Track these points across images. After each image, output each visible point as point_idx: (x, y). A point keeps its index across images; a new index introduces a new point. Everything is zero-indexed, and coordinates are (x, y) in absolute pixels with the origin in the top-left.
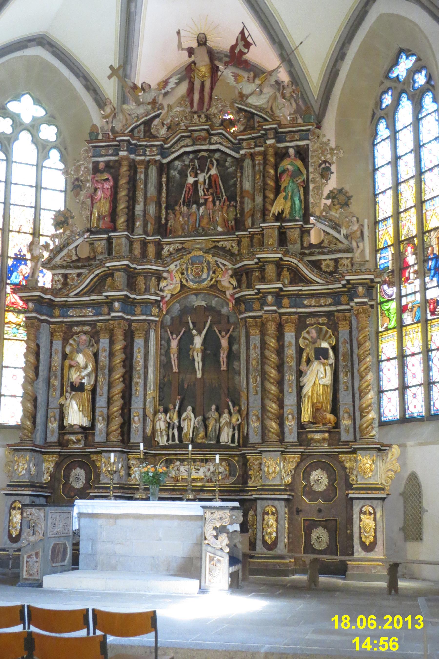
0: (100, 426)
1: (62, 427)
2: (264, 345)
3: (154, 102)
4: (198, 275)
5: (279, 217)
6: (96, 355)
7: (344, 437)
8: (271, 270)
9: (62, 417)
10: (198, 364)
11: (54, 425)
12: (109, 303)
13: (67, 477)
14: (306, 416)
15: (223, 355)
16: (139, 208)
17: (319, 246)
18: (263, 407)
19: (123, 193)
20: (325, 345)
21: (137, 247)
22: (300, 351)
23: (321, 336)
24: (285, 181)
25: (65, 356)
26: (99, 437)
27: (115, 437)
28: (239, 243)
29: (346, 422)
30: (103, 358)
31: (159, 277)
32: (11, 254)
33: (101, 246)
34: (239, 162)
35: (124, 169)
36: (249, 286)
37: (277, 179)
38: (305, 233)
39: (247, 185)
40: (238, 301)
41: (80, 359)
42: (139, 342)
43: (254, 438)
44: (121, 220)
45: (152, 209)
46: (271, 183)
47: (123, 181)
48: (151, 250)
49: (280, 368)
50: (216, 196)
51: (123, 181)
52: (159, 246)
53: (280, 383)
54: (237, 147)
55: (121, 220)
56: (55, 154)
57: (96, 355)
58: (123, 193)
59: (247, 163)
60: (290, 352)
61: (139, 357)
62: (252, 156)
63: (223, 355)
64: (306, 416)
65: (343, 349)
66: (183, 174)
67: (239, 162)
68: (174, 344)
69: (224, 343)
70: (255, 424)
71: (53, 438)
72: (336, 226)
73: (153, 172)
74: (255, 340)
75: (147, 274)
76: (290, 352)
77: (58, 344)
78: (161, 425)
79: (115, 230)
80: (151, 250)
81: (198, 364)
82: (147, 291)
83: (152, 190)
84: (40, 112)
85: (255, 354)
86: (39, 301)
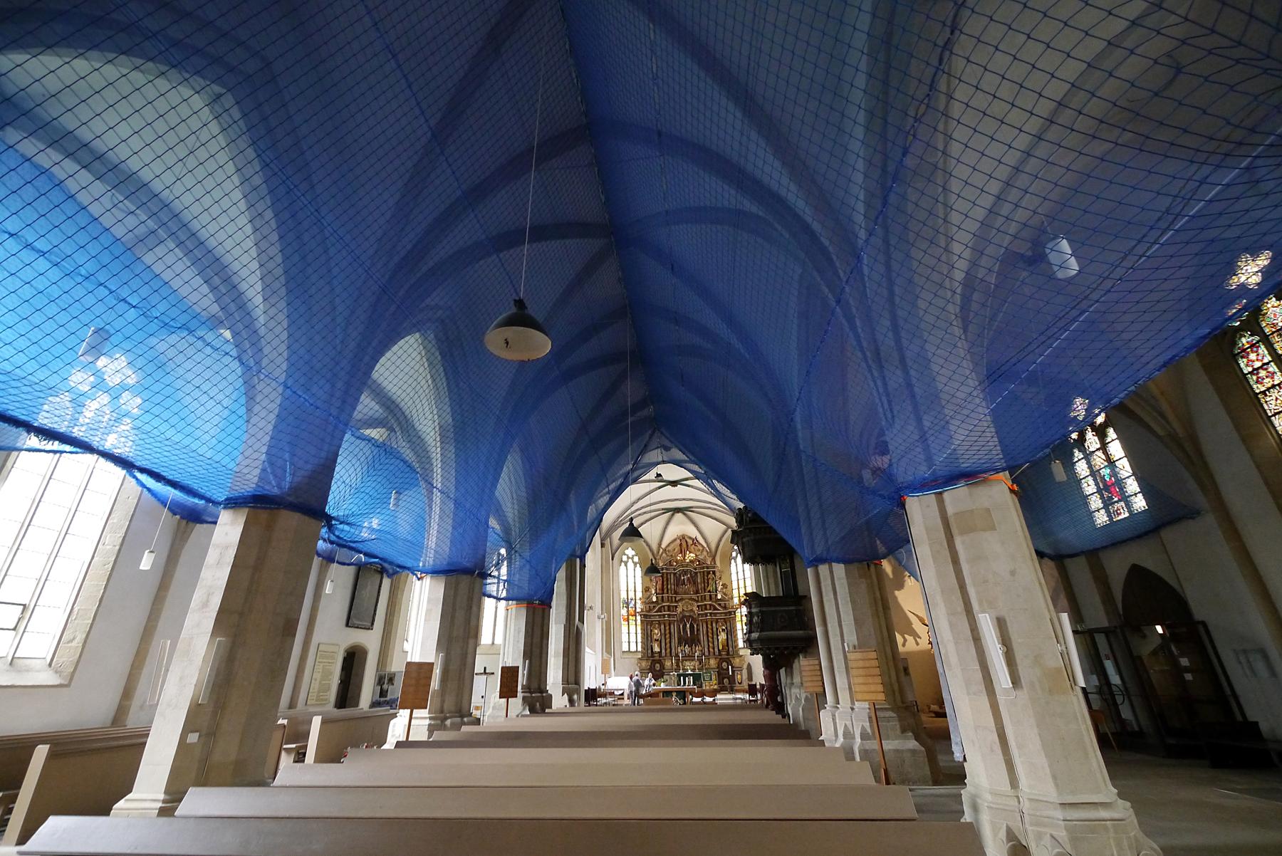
0: (663, 651)
1: (652, 651)
2: (707, 627)
3: (672, 555)
4: (687, 606)
5: (709, 591)
6: (660, 630)
7: (731, 653)
8: (708, 607)
9: (652, 648)
10: (689, 633)
11: (650, 651)
12: (664, 615)
13: (654, 666)
14: (721, 648)
15: (695, 630)
16: (669, 586)
17: (720, 599)
18: (709, 646)
19: (665, 583)
20: (724, 628)
21: (670, 598)
22: (717, 629)
23: (723, 625)
24: (710, 581)
25: (651, 631)
26: (663, 654)
27: (668, 655)
28: (698, 597)
29: (731, 649)
30: (663, 631)
31: (676, 607)
32: (629, 598)
33: (660, 598)
34: (696, 573)
35: (665, 575)
36: (702, 611)
37: (708, 580)
38: (716, 595)
39: (699, 581)
40: (699, 614)
41: (656, 631)
42: (672, 626)
43: (707, 654)
44: (665, 591)
45: (673, 587)
46: (706, 581)
47: (665, 579)
48: (674, 598)
49: (713, 634)
50: (690, 583)
51: (665, 579)
52: (675, 597)
53: (713, 638)
54: (695, 569)
55: (665, 591)
56: (638, 565)
57: (660, 630)
58: (665, 583)
59: (699, 574)
60: (715, 629)
61: (672, 631)
62: (700, 572)
63: (695, 630)
64: (721, 648)
65: (729, 628)
66: (680, 576)
67: (696, 573)
68: (681, 626)
69: (695, 626)
70: (706, 650)
71: (650, 655)
72: (725, 594)
73: (672, 576)
74: (705, 626)
75: (673, 606)
76: (715, 629)
77: (649, 627)
78: (679, 651)
79: (663, 593)
80: (674, 598)
81: (689, 633)
82: (673, 611)
83: (672, 581)
84: (633, 553)
85: (705, 630)
86: (644, 615)
